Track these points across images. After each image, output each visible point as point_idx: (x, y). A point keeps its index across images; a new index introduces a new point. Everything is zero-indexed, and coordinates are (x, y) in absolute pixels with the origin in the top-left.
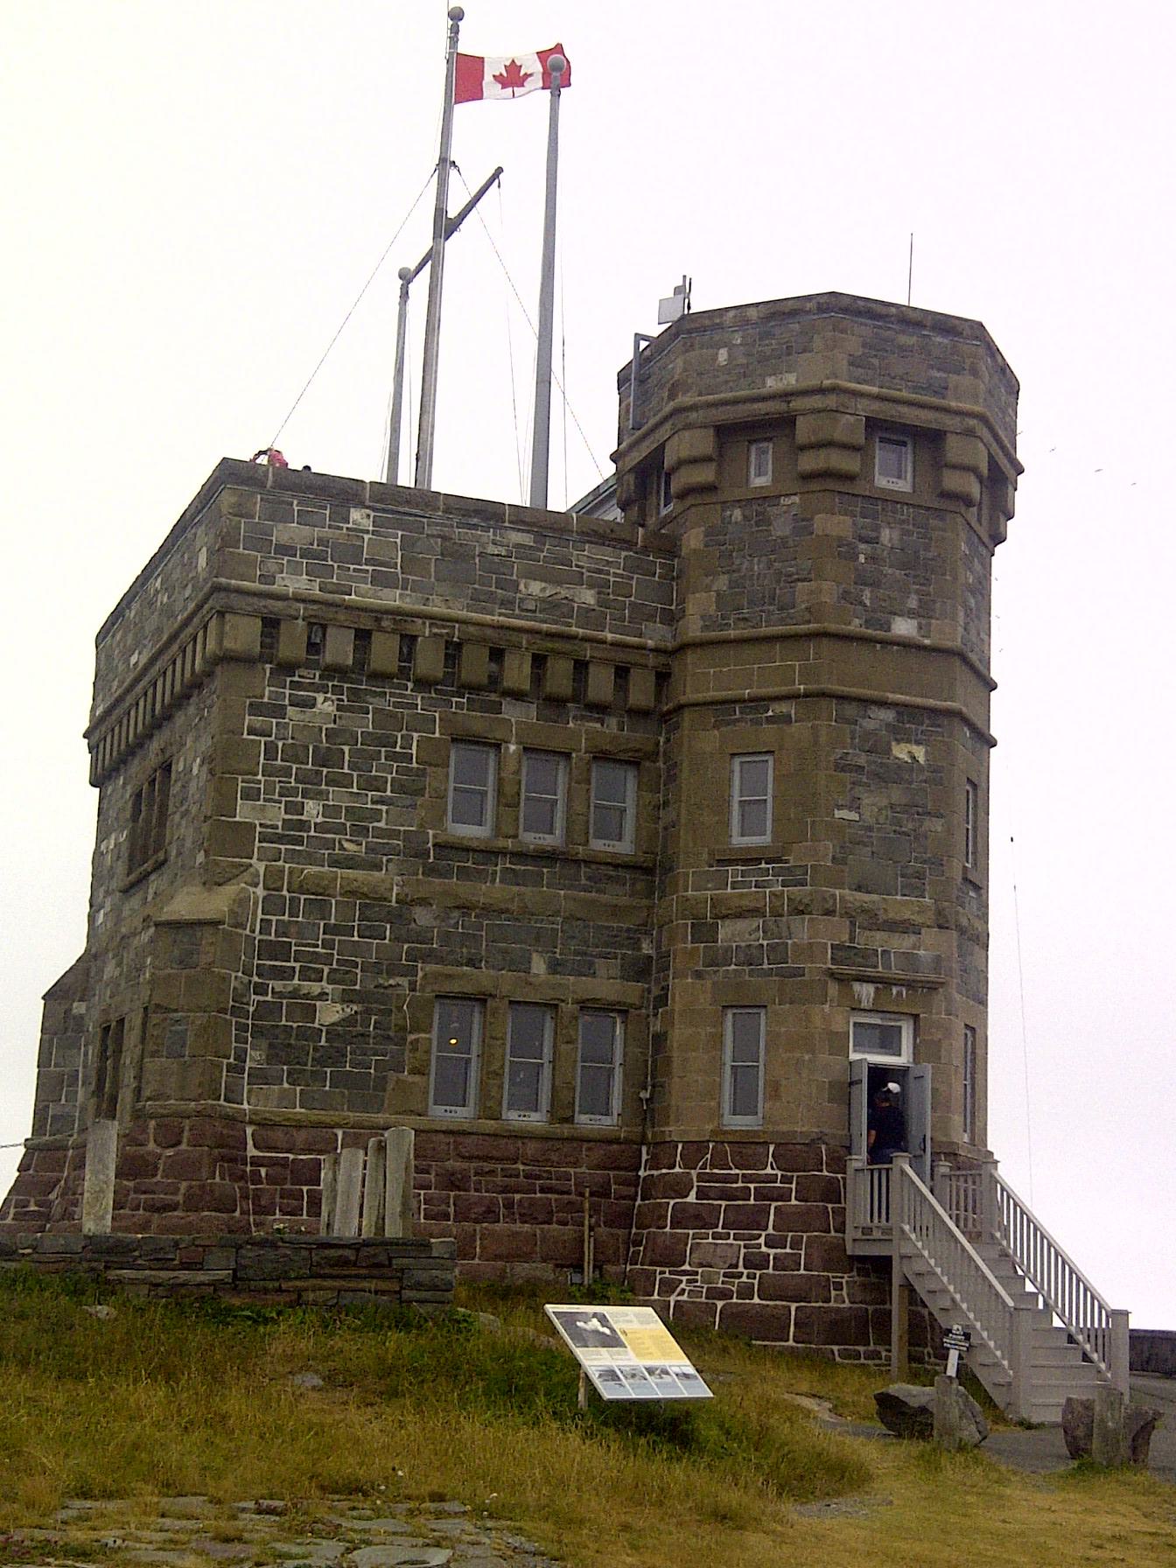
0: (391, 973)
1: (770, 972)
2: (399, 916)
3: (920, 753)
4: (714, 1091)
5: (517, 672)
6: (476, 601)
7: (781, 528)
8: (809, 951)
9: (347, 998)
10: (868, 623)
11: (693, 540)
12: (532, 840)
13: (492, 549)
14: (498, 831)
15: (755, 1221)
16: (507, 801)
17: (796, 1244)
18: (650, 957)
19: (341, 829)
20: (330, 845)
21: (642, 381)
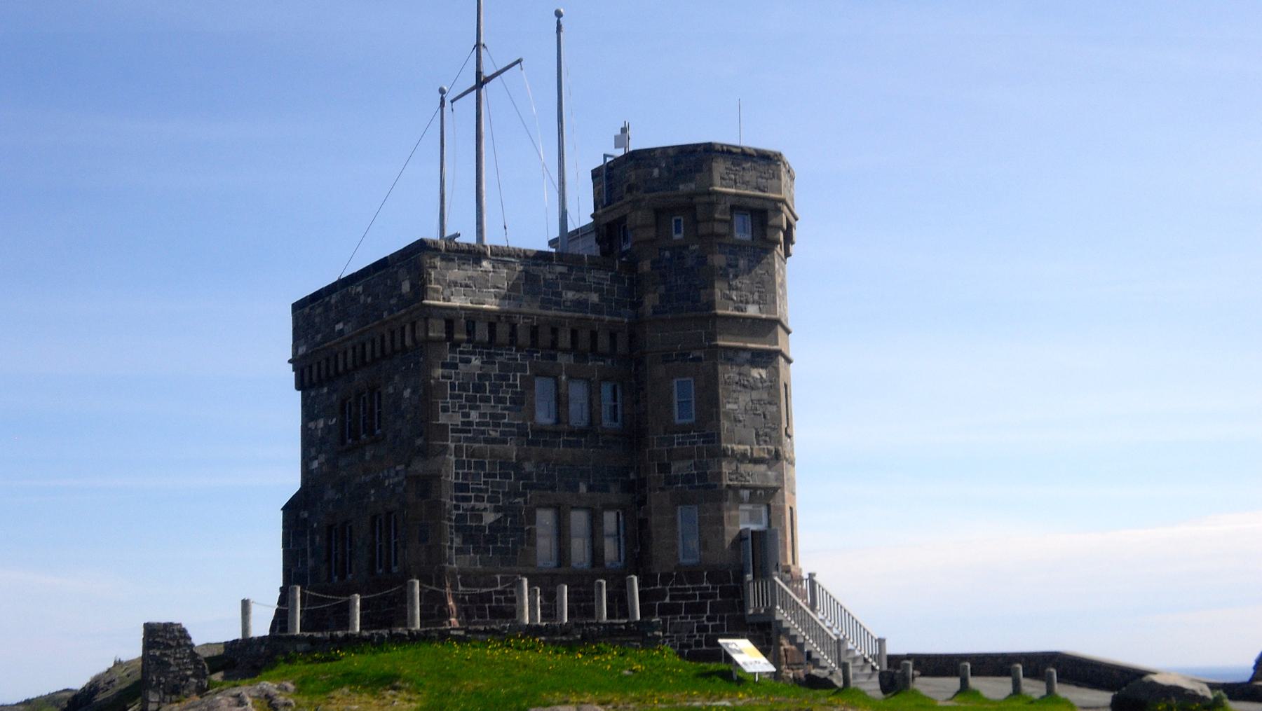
0: (517, 495)
1: (699, 487)
2: (517, 467)
3: (764, 373)
5: (565, 340)
9: (497, 510)
13: (549, 276)
15: (700, 609)
17: (722, 619)
18: (633, 481)
19: (487, 424)
20: (483, 433)
21: (609, 178)
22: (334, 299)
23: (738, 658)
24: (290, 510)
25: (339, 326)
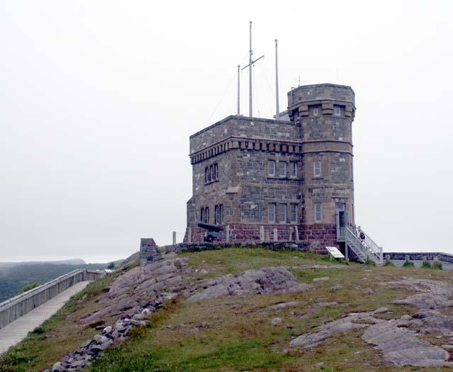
4: (313, 217)
5: (278, 149)
6: (272, 136)
7: (320, 123)
8: (328, 194)
9: (255, 204)
10: (335, 139)
11: (304, 124)
12: (282, 176)
14: (276, 175)
16: (277, 170)
22: (203, 135)
23: (332, 253)
24: (189, 202)
25: (204, 144)
